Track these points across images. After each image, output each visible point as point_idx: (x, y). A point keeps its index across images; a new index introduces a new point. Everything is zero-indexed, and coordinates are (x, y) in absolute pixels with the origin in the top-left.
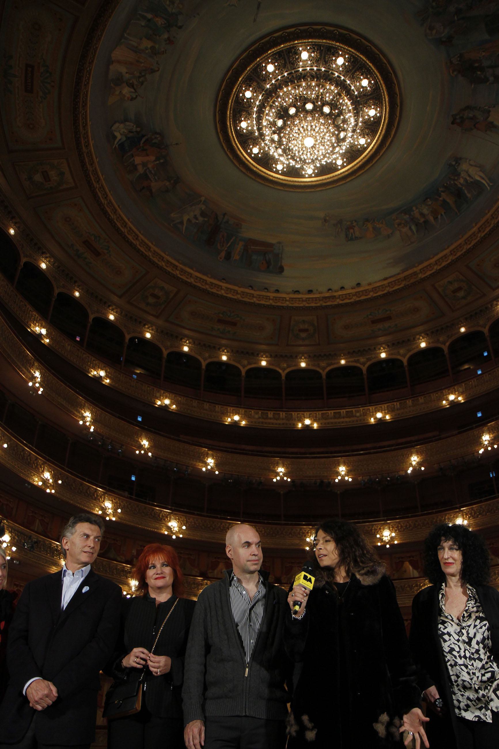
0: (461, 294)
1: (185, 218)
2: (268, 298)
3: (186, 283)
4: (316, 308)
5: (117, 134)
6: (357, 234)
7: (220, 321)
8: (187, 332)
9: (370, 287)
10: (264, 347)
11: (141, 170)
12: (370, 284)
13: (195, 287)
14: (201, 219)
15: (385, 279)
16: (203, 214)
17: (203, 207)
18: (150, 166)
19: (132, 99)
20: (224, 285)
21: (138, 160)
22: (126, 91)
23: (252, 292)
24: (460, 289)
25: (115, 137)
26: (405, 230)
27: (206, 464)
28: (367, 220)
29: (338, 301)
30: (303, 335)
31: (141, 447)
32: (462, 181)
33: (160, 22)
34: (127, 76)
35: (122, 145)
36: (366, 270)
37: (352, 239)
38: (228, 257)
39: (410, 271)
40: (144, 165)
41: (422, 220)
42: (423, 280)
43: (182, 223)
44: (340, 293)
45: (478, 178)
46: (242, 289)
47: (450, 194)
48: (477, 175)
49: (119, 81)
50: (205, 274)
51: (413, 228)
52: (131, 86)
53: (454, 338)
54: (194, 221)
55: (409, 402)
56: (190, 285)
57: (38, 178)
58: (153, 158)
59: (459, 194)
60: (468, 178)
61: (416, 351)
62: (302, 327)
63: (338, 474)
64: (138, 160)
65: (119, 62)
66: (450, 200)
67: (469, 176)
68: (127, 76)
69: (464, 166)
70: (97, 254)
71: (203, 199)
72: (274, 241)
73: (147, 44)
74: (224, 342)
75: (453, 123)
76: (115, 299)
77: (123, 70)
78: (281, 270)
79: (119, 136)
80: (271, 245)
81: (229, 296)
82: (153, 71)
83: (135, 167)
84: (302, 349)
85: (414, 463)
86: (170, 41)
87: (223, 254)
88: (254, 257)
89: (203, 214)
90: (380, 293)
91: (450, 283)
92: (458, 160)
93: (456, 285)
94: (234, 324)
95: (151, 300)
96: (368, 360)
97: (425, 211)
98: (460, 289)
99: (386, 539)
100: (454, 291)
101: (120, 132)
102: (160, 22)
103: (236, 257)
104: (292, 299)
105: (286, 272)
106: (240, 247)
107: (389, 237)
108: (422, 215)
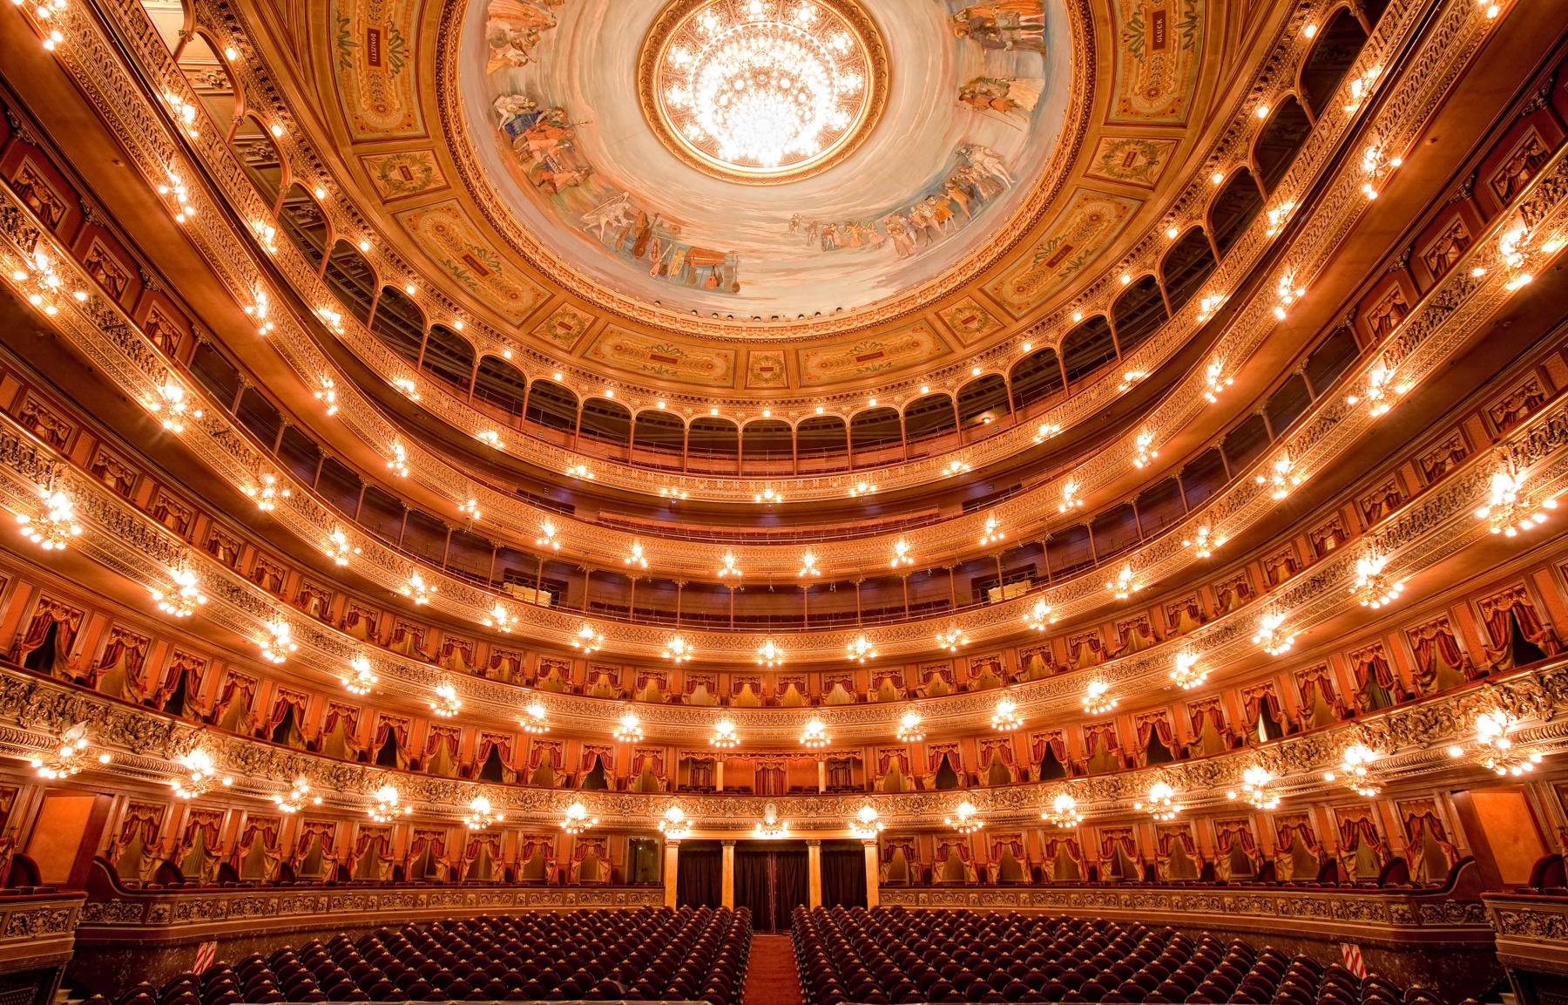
0: (974, 325)
1: (603, 221)
2: (717, 327)
3: (606, 309)
4: (783, 341)
5: (502, 111)
6: (838, 241)
7: (653, 357)
8: (611, 372)
9: (854, 315)
10: (715, 391)
11: (538, 158)
12: (854, 310)
13: (618, 314)
14: (624, 222)
15: (875, 303)
16: (627, 215)
17: (627, 206)
18: (551, 152)
19: (521, 64)
20: (658, 311)
21: (533, 145)
22: (512, 53)
23: (696, 319)
24: (973, 318)
25: (500, 116)
26: (902, 237)
27: (631, 554)
28: (850, 224)
29: (812, 332)
30: (767, 375)
31: (543, 534)
32: (975, 175)
34: (512, 34)
35: (510, 126)
36: (853, 290)
37: (830, 248)
38: (664, 271)
39: (908, 294)
40: (542, 150)
41: (924, 225)
42: (923, 307)
43: (598, 227)
44: (815, 320)
46: (683, 316)
48: (995, 169)
49: (501, 40)
50: (632, 296)
51: (912, 234)
53: (965, 382)
54: (615, 224)
55: (902, 470)
56: (612, 312)
57: (395, 175)
58: (555, 142)
59: (971, 193)
61: (916, 397)
62: (764, 365)
63: (803, 565)
65: (499, 16)
66: (961, 200)
68: (512, 34)
69: (978, 156)
70: (483, 272)
74: (661, 384)
75: (961, 99)
76: (511, 330)
77: (505, 26)
78: (736, 288)
79: (506, 115)
80: (722, 255)
81: (666, 325)
82: (547, 27)
83: (530, 155)
84: (766, 393)
85: (900, 553)
87: (657, 268)
88: (699, 271)
89: (627, 215)
90: (867, 322)
91: (959, 310)
92: (969, 147)
93: (967, 314)
94: (674, 361)
95: (561, 331)
96: (853, 408)
97: (928, 214)
98: (973, 318)
99: (861, 651)
100: (966, 321)
101: (507, 109)
103: (673, 270)
104: (749, 329)
105: (744, 291)
106: (678, 259)
107: (879, 246)
108: (924, 218)
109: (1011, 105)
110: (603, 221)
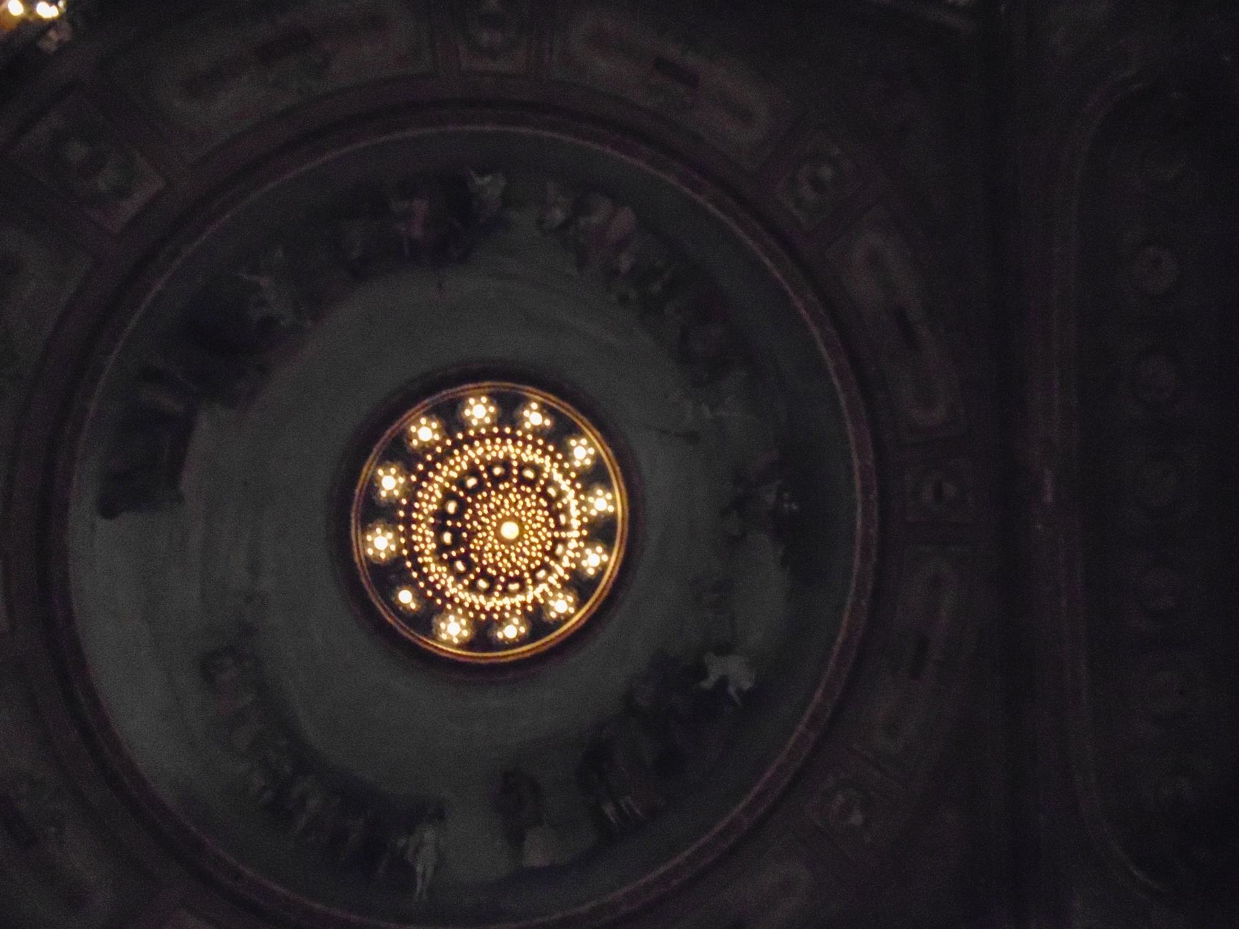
1: (264, 281)
5: (487, 179)
19: (540, 222)
21: (420, 206)
22: (558, 215)
25: (482, 174)
32: (402, 842)
33: (656, 288)
45: (419, 869)
47: (367, 832)
48: (423, 866)
51: (268, 795)
52: (565, 225)
58: (417, 233)
60: (410, 851)
64: (420, 206)
67: (417, 851)
69: (429, 835)
71: (309, 324)
72: (189, 480)
73: (625, 263)
77: (595, 220)
79: (479, 181)
86: (624, 300)
97: (313, 803)
101: (489, 186)
102: (656, 288)
109: (516, 839)
110: (264, 281)
